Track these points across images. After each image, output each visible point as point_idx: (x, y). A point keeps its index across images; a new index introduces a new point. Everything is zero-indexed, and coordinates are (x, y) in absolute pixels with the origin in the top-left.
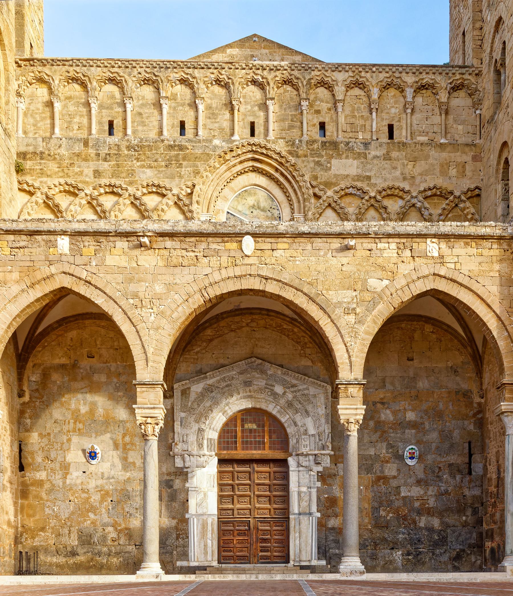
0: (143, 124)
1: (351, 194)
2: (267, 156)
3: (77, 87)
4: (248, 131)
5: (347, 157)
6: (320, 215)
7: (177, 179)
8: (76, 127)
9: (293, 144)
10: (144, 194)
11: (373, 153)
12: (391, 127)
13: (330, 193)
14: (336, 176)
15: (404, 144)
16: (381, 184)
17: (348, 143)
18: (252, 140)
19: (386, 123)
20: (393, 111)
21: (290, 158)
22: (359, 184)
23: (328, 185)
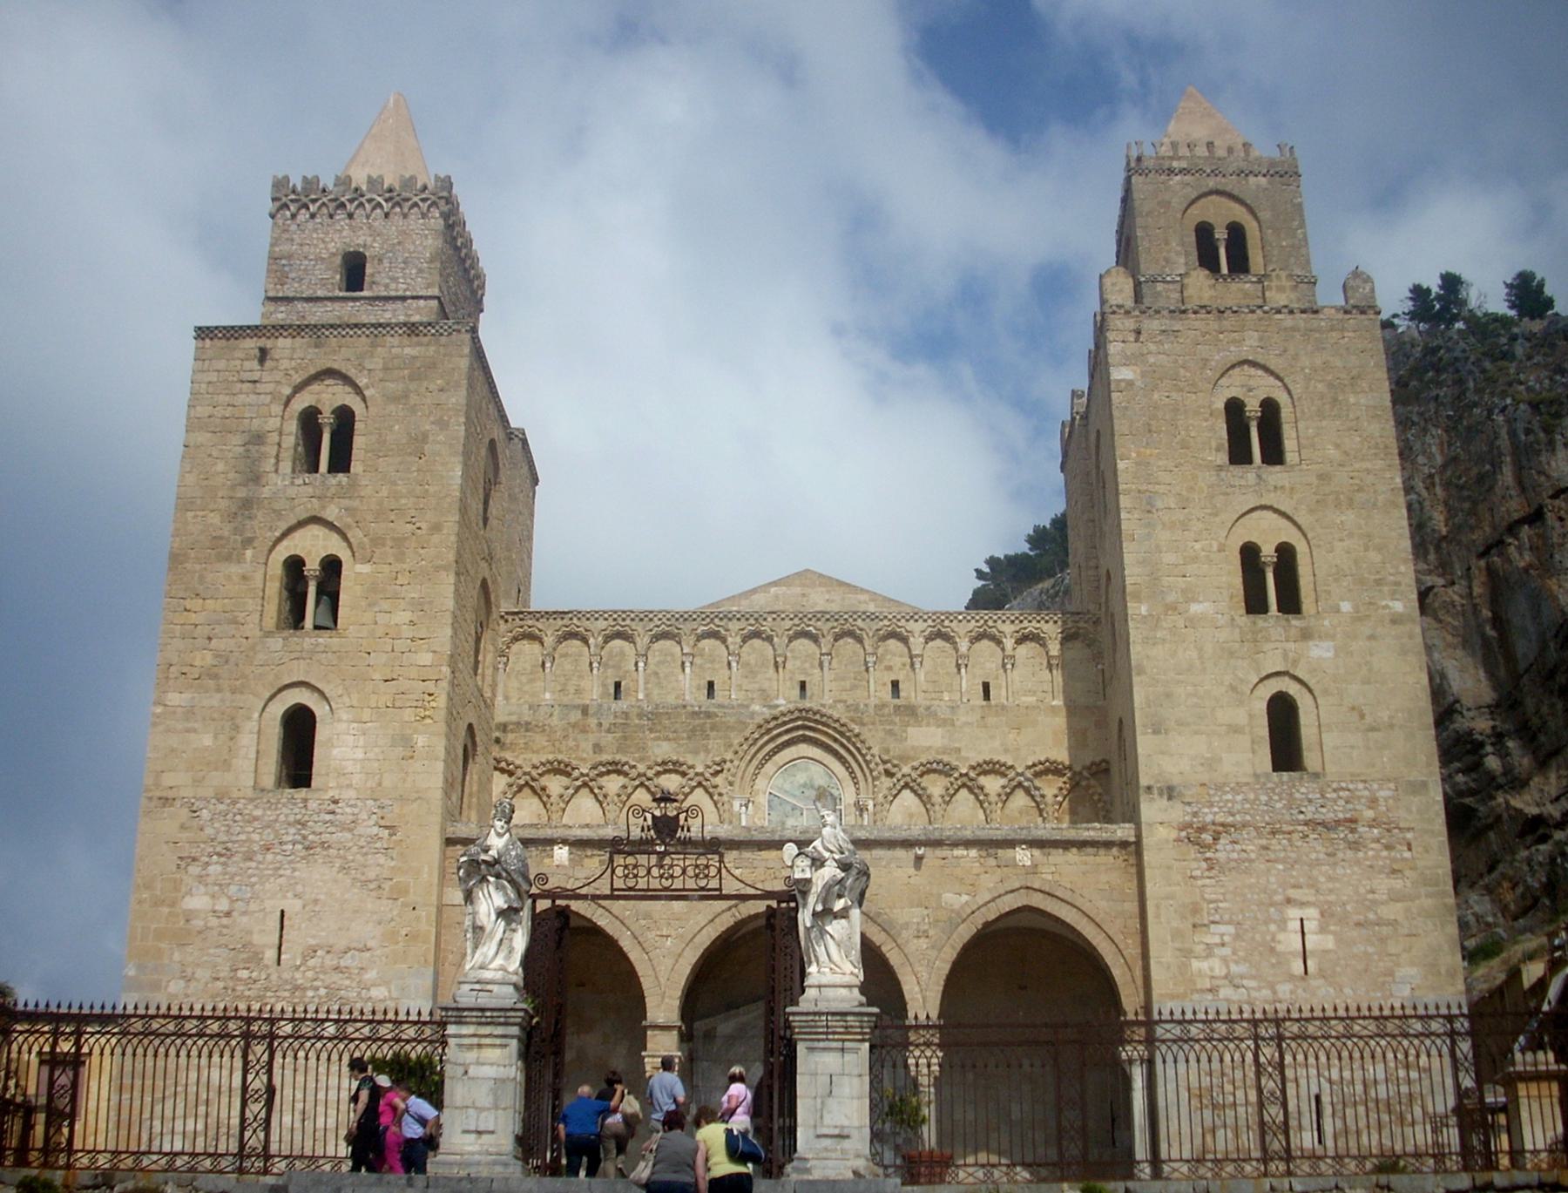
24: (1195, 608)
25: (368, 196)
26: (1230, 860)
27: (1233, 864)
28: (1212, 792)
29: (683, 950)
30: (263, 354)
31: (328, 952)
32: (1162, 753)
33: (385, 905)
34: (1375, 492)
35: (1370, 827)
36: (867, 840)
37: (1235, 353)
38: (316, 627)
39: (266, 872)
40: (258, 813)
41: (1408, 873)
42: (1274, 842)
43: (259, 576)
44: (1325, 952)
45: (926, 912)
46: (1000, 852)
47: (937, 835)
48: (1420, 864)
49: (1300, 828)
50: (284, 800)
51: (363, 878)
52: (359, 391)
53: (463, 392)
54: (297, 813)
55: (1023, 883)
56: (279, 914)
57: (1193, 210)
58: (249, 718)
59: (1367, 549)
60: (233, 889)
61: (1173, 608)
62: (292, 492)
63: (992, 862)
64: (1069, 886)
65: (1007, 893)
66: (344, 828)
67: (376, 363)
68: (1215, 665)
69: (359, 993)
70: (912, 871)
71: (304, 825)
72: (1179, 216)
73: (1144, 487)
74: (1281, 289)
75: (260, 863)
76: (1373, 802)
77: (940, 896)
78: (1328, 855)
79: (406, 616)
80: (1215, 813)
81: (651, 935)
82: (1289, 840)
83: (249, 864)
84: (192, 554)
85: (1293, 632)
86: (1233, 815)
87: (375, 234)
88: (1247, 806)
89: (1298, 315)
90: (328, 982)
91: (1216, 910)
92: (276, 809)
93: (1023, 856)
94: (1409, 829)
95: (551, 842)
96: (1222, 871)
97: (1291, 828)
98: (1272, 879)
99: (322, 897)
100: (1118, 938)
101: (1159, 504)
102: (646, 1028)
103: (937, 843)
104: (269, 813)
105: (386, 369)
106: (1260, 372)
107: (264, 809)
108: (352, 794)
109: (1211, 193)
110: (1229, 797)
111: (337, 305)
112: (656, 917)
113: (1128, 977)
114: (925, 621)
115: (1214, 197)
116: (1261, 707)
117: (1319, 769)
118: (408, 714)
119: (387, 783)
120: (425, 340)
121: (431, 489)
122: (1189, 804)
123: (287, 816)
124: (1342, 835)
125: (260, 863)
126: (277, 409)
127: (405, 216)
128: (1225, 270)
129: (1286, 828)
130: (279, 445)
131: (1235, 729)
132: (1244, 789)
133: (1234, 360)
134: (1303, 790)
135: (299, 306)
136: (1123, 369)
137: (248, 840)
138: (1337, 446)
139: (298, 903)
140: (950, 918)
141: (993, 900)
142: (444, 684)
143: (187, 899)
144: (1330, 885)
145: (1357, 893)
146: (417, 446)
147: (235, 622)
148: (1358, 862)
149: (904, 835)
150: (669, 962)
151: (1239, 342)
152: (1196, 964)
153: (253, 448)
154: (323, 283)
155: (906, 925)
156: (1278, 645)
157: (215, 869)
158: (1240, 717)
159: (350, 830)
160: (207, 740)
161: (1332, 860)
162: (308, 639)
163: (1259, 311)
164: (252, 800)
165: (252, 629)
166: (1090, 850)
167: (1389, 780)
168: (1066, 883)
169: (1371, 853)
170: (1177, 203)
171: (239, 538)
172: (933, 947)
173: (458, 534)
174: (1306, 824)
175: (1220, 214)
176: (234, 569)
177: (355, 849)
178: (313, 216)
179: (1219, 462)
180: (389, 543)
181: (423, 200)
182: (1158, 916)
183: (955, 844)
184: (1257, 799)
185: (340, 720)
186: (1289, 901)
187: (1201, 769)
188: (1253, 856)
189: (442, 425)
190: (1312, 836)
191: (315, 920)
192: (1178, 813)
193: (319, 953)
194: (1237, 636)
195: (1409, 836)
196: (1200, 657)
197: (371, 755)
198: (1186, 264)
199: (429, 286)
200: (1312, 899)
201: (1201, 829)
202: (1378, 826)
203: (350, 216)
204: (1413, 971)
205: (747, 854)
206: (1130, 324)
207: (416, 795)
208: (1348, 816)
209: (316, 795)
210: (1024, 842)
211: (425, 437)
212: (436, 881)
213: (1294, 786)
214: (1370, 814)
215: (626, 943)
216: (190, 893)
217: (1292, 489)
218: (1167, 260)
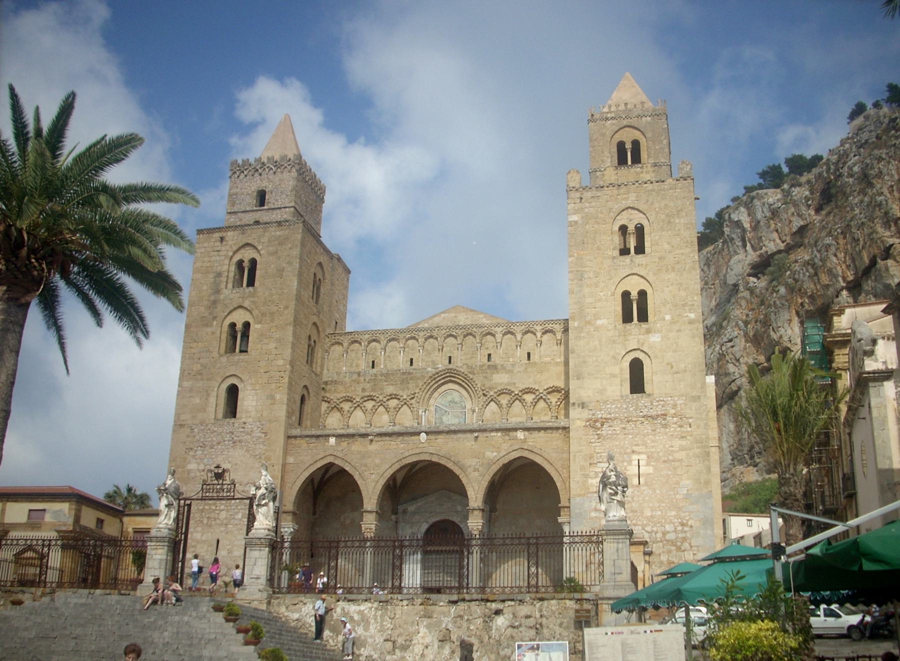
0: (390, 361)
1: (505, 393)
2: (459, 375)
3: (357, 345)
4: (448, 361)
5: (502, 373)
6: (487, 405)
7: (406, 391)
8: (354, 365)
9: (472, 368)
10: (388, 400)
11: (517, 370)
12: (529, 354)
13: (492, 393)
14: (495, 384)
15: (535, 363)
16: (522, 387)
17: (502, 366)
18: (448, 367)
19: (526, 352)
20: (530, 345)
21: (470, 375)
22: (509, 388)
23: (491, 389)
24: (599, 322)
25: (267, 165)
26: (608, 434)
27: (610, 436)
30: (222, 239)
32: (580, 388)
34: (685, 263)
35: (673, 417)
37: (625, 204)
38: (241, 351)
41: (689, 438)
43: (218, 332)
44: (650, 474)
46: (511, 434)
47: (484, 427)
48: (695, 433)
52: (258, 251)
53: (299, 249)
55: (520, 447)
57: (617, 136)
58: (213, 391)
59: (679, 290)
60: (206, 460)
61: (589, 323)
62: (231, 296)
63: (507, 438)
67: (265, 240)
70: (473, 443)
72: (609, 139)
73: (579, 269)
74: (647, 172)
76: (675, 406)
77: (484, 453)
78: (653, 431)
79: (274, 345)
81: (366, 473)
84: (194, 324)
85: (643, 330)
87: (269, 181)
89: (655, 184)
91: (601, 456)
93: (520, 435)
94: (691, 418)
95: (329, 436)
96: (604, 440)
98: (626, 442)
100: (560, 469)
101: (586, 276)
103: (485, 430)
105: (269, 241)
106: (636, 212)
108: (251, 420)
109: (625, 127)
111: (254, 213)
113: (564, 487)
115: (627, 129)
117: (651, 392)
118: (273, 386)
119: (264, 415)
120: (285, 228)
121: (285, 291)
122: (591, 410)
126: (227, 262)
127: (282, 172)
128: (630, 163)
129: (634, 419)
130: (228, 276)
131: (613, 376)
133: (623, 207)
135: (240, 215)
136: (574, 216)
137: (212, 441)
138: (669, 243)
140: (488, 463)
141: (507, 454)
142: (287, 373)
143: (189, 465)
144: (653, 444)
145: (664, 447)
146: (280, 272)
147: (209, 351)
148: (666, 434)
149: (471, 427)
150: (373, 484)
151: (627, 199)
152: (590, 481)
153: (217, 279)
154: (249, 204)
155: (470, 466)
156: (635, 337)
157: (199, 452)
158: (616, 370)
159: (250, 435)
160: (197, 401)
161: (654, 433)
162: (238, 357)
163: (637, 184)
164: (213, 424)
165: (215, 354)
166: (550, 431)
167: (683, 396)
169: (672, 429)
170: (609, 134)
171: (211, 317)
173: (295, 309)
174: (643, 417)
175: (627, 137)
176: (209, 330)
178: (246, 176)
179: (614, 255)
180: (268, 315)
181: (289, 165)
182: (574, 460)
183: (492, 431)
184: (621, 406)
186: (633, 452)
187: (597, 394)
188: (618, 432)
189: (290, 263)
192: (586, 414)
194: (617, 333)
195: (690, 421)
197: (258, 404)
198: (611, 161)
199: (290, 202)
200: (644, 450)
201: (596, 421)
202: (677, 417)
203: (260, 174)
204: (688, 482)
205: (406, 438)
206: (578, 195)
208: (663, 413)
210: (521, 429)
211: (283, 269)
212: (281, 454)
214: (673, 411)
216: (189, 463)
217: (646, 265)
218: (602, 161)
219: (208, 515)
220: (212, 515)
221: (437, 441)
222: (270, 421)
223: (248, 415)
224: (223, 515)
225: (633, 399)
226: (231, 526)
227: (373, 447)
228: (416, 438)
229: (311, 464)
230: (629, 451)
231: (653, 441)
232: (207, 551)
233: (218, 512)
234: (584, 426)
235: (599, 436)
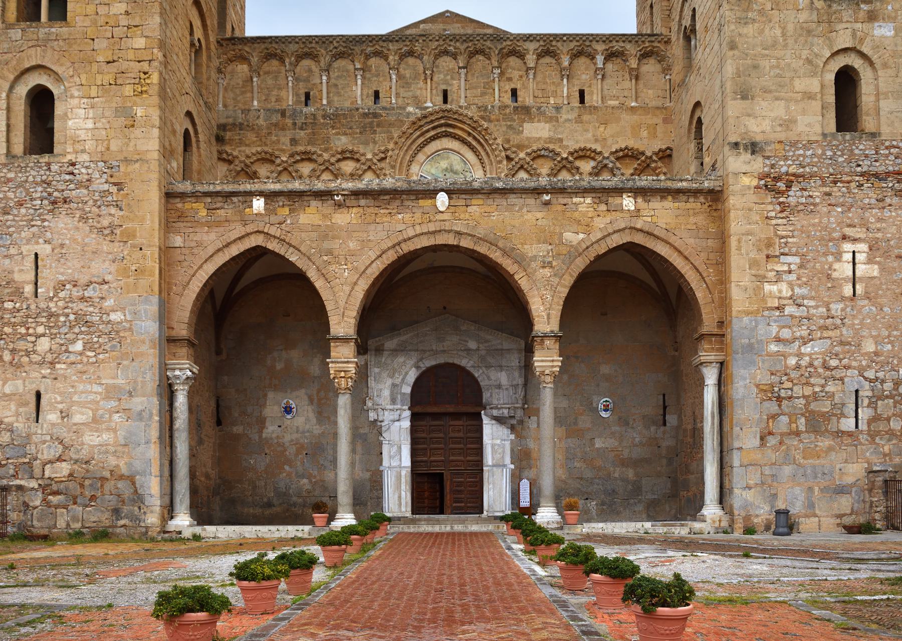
27: (801, 207)
28: (787, 148)
29: (358, 279)
31: (75, 286)
33: (116, 247)
36: (504, 189)
39: (21, 223)
40: (11, 175)
42: (835, 189)
45: (550, 247)
49: (857, 178)
50: (31, 165)
51: (99, 226)
54: (43, 174)
55: (629, 224)
56: (33, 256)
63: (603, 207)
64: (664, 227)
65: (615, 232)
66: (79, 185)
68: (796, 42)
69: (101, 317)
71: (49, 184)
75: (15, 216)
80: (789, 166)
82: (848, 188)
83: (6, 217)
86: (804, 167)
88: (816, 160)
90: (76, 309)
92: (25, 172)
93: (628, 202)
97: (849, 178)
99: (67, 242)
100: (702, 268)
102: (329, 339)
104: (20, 175)
107: (16, 173)
108: (85, 157)
110: (801, 152)
112: (336, 253)
114: (538, 41)
116: (831, 77)
119: (113, 147)
122: (768, 158)
123: (34, 177)
124: (891, 185)
125: (15, 216)
129: (845, 178)
132: (814, 146)
134: (861, 147)
139: (48, 248)
140: (569, 252)
141: (604, 238)
150: (347, 289)
168: (662, 223)
172: (555, 275)
174: (862, 174)
177: (91, 203)
184: (824, 153)
185: (72, 97)
187: (779, 129)
188: (818, 200)
190: (866, 185)
191: (62, 261)
192: (758, 165)
193: (68, 287)
196: (783, 35)
207: (138, 157)
208: (896, 169)
209: (56, 159)
213: (854, 144)
215: (312, 274)
219: (11, 346)
220: (21, 345)
221: (470, 209)
222: (126, 160)
223: (79, 147)
224: (44, 344)
225: (845, 141)
226: (63, 366)
227: (342, 218)
228: (425, 203)
229: (219, 250)
230: (836, 235)
231: (879, 220)
232: (18, 414)
233: (33, 339)
234: (757, 187)
235: (784, 207)
